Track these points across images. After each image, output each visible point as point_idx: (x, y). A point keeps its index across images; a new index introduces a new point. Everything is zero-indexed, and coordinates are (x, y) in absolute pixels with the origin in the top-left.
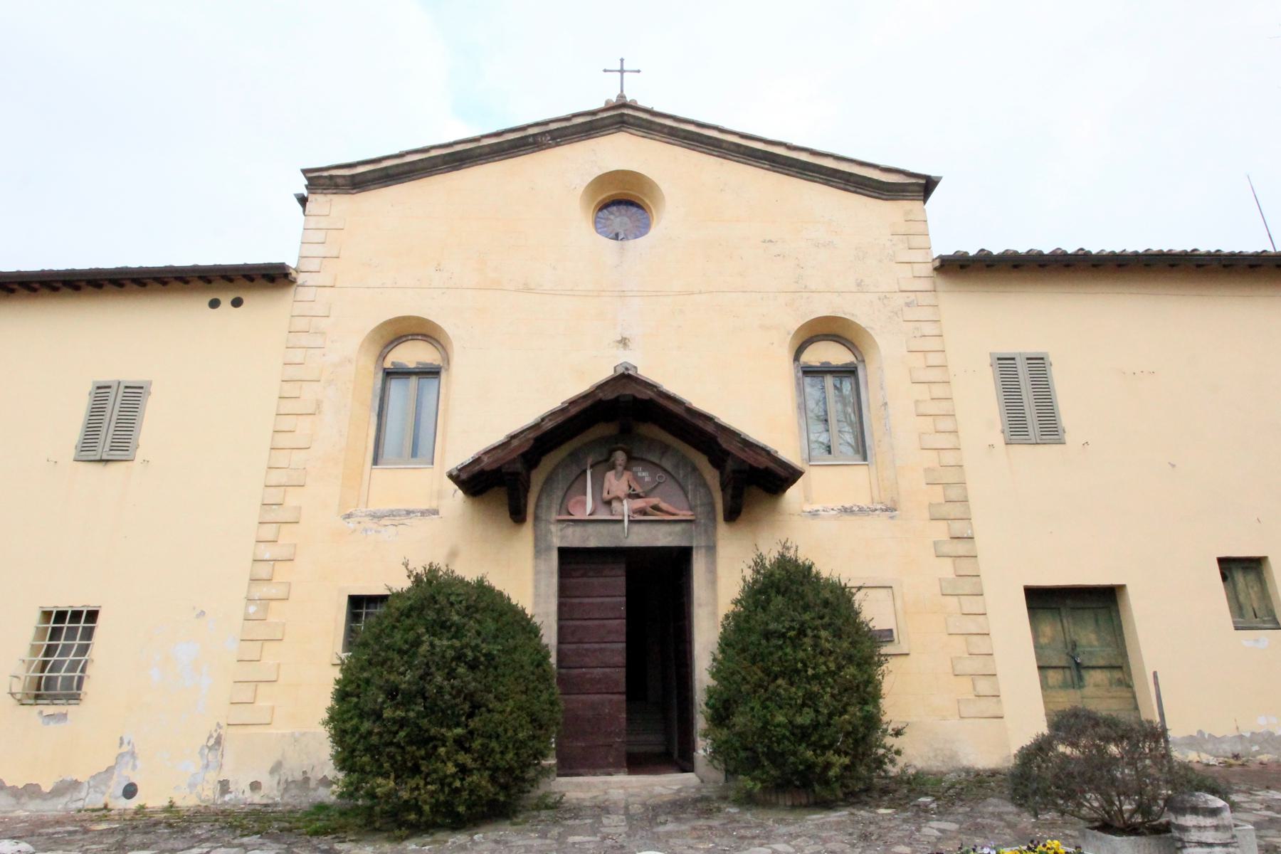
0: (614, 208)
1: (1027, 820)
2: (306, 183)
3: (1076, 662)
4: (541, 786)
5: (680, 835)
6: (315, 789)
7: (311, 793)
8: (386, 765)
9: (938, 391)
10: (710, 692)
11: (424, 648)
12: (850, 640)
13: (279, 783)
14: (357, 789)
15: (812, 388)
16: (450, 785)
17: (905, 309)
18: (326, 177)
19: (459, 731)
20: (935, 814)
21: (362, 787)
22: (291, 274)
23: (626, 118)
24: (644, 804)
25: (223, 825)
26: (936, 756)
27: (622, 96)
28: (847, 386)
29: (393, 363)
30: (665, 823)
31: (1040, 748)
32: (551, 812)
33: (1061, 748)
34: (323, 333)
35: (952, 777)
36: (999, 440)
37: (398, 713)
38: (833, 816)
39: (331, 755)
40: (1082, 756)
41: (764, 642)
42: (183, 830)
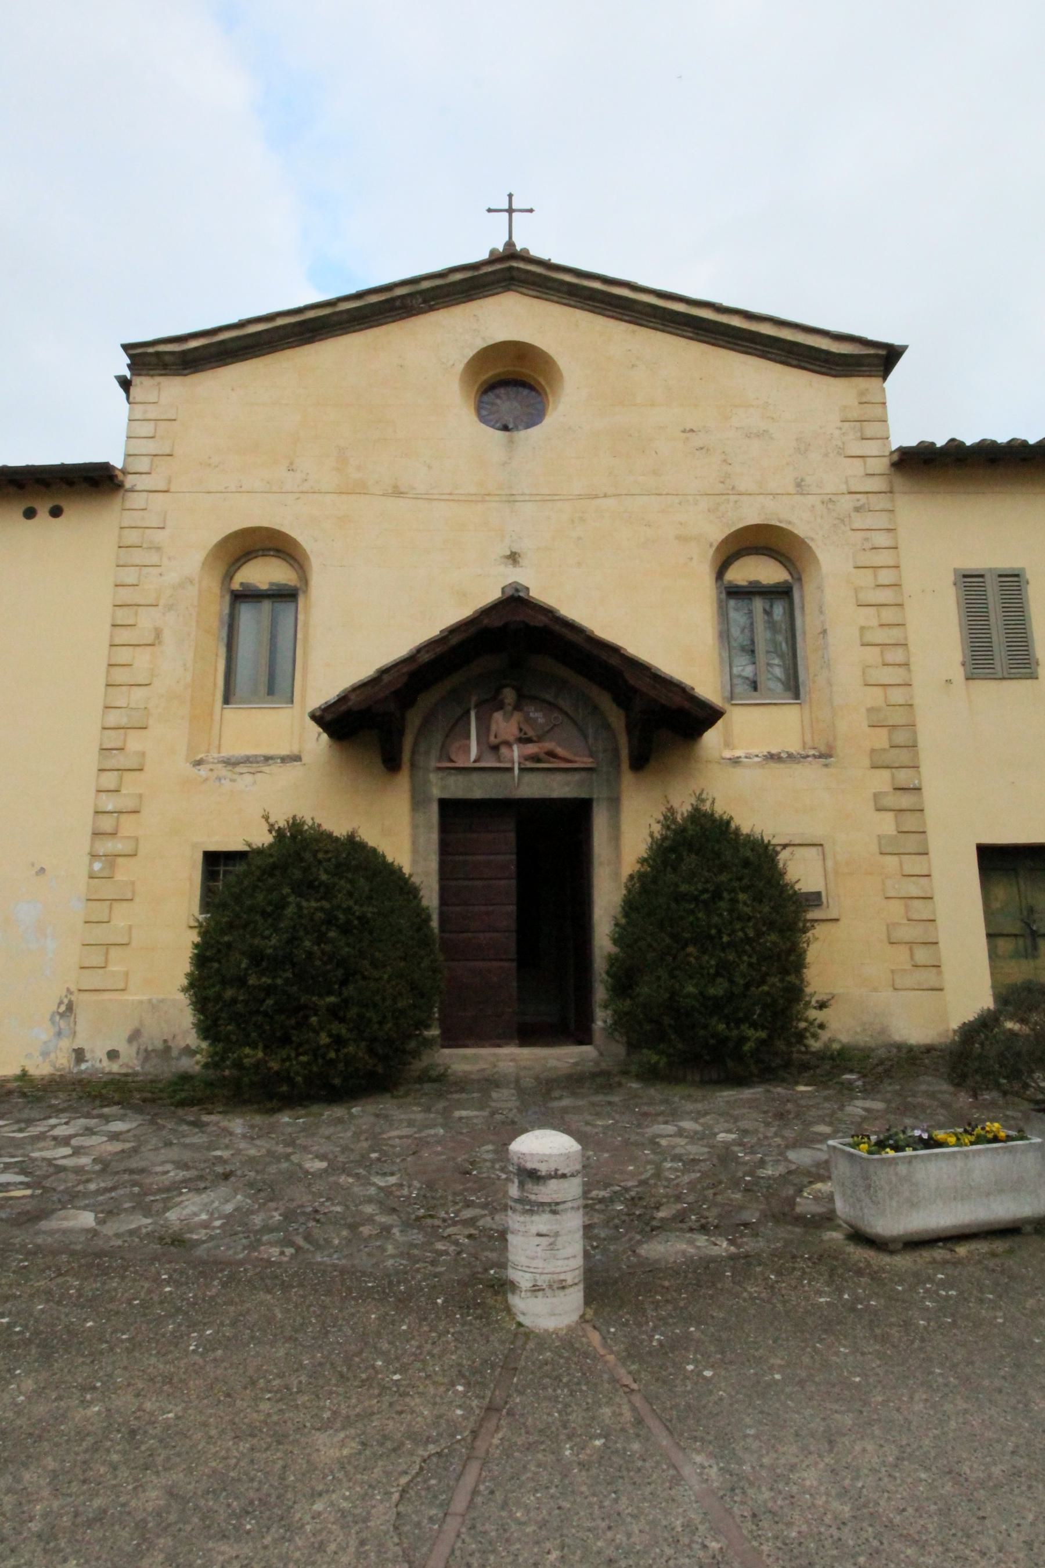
0: (502, 391)
1: (964, 1099)
2: (129, 362)
3: (1031, 929)
4: (424, 1057)
5: (577, 1110)
6: (178, 1059)
7: (174, 1063)
8: (254, 1035)
9: (889, 615)
10: (612, 960)
11: (290, 910)
12: (772, 904)
13: (138, 1053)
14: (223, 1059)
15: (737, 616)
16: (323, 1057)
17: (853, 514)
18: (151, 354)
19: (332, 999)
20: (860, 1092)
21: (228, 1057)
22: (116, 476)
23: (515, 273)
24: (537, 1078)
25: (81, 1094)
26: (864, 1030)
27: (510, 244)
28: (779, 611)
29: (242, 584)
30: (560, 1098)
31: (985, 1023)
32: (436, 1085)
33: (1009, 1025)
34: (158, 549)
35: (882, 1053)
36: (958, 673)
37: (263, 980)
38: (747, 1093)
39: (193, 1024)
40: (1032, 1033)
41: (673, 905)
42: (39, 1099)
